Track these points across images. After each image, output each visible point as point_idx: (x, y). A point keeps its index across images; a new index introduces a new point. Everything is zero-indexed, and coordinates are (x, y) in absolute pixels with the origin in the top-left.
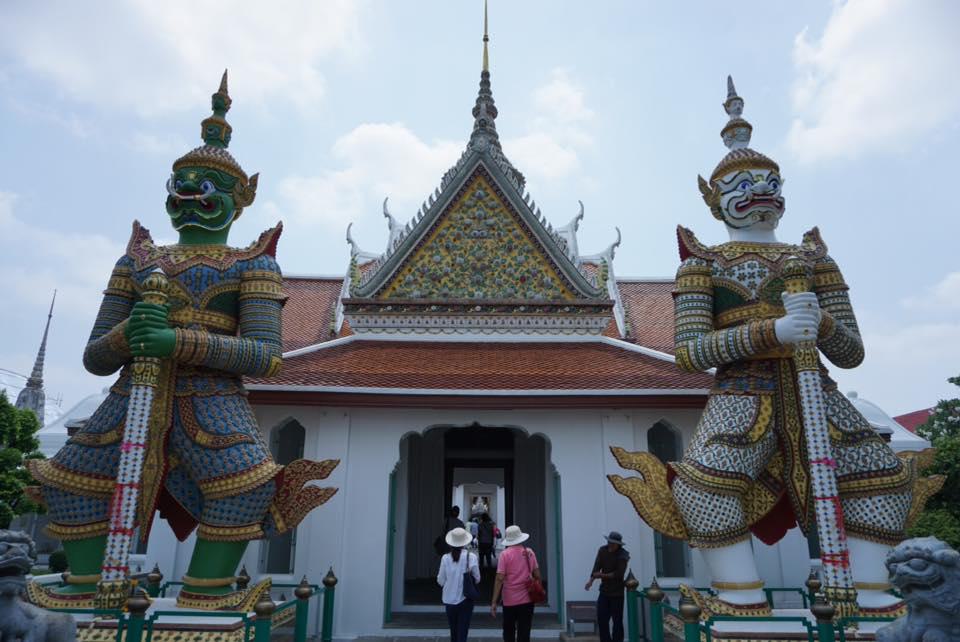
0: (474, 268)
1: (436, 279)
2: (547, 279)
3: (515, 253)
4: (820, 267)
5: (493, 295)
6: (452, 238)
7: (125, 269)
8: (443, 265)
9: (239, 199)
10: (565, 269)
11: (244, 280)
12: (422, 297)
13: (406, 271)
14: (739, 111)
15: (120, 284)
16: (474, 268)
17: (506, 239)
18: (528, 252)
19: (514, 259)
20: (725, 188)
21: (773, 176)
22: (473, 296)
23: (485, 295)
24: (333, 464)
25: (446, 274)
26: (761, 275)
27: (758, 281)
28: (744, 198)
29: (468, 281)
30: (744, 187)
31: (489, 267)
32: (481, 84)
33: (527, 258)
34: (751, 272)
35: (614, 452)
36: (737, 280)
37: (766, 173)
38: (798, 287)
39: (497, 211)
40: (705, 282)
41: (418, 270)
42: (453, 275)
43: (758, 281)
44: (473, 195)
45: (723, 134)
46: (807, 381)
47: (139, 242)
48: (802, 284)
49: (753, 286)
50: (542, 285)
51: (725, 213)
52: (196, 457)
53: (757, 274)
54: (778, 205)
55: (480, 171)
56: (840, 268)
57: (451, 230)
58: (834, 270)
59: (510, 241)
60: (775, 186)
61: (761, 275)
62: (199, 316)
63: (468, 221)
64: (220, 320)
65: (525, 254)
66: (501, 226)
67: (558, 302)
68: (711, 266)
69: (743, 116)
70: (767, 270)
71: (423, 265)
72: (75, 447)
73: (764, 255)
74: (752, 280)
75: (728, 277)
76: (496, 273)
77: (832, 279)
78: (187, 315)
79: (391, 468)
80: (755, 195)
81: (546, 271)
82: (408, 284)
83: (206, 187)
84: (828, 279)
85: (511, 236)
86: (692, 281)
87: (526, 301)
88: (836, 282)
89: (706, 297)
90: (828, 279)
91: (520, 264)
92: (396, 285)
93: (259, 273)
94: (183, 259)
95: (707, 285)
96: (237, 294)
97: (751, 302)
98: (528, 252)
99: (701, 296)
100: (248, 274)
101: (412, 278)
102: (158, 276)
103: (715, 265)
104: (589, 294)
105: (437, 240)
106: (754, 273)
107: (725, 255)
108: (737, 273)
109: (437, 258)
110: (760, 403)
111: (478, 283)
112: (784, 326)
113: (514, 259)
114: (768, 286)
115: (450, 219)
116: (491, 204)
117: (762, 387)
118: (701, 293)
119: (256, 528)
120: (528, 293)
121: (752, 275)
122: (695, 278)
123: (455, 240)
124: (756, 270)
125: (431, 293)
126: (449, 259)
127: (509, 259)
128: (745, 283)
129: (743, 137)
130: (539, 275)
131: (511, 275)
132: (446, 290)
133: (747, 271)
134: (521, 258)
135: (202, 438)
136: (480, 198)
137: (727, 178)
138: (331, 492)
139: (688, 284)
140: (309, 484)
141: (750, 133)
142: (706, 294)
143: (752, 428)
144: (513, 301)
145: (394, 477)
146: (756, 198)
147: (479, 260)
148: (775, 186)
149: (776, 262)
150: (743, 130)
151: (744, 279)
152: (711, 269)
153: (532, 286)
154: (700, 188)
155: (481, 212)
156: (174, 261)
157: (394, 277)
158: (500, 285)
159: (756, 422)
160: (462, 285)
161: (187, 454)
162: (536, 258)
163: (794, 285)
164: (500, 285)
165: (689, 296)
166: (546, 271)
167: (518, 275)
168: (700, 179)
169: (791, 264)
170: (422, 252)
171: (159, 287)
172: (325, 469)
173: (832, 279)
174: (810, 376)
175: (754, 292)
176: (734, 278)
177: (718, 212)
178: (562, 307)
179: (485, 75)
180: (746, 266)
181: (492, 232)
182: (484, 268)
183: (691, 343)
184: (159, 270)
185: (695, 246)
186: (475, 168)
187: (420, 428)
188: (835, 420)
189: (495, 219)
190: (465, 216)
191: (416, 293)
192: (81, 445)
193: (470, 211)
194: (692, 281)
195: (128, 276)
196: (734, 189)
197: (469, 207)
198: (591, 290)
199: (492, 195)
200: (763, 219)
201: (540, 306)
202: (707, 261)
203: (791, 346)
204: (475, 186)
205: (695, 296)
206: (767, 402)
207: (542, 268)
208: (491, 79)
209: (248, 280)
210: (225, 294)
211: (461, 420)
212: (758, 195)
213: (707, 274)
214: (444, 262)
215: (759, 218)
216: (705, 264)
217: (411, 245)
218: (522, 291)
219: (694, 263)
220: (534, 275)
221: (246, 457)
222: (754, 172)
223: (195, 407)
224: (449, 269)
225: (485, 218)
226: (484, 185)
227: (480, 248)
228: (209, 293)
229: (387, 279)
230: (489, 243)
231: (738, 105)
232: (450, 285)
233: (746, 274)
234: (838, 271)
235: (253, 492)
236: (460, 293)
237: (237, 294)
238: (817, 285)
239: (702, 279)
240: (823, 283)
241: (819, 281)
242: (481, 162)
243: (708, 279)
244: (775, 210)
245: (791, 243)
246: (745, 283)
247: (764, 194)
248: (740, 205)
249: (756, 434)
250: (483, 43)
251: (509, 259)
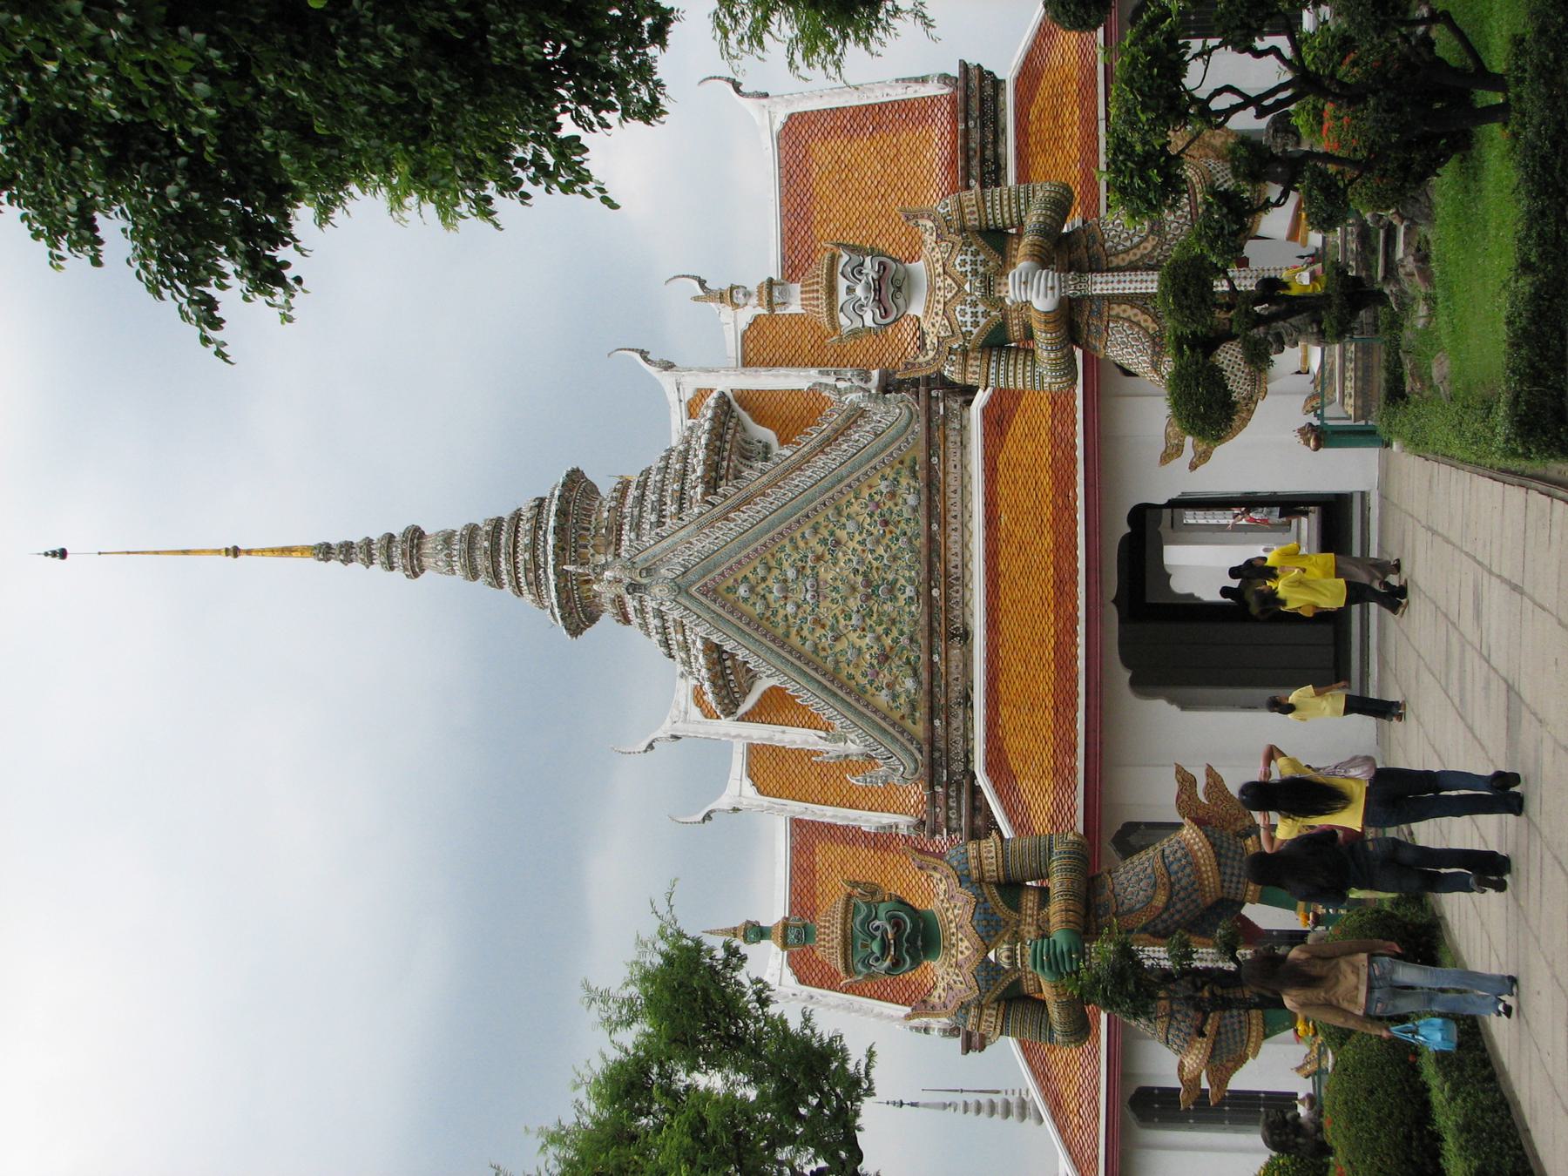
0: (868, 597)
1: (884, 658)
2: (883, 486)
4: (956, 225)
5: (910, 568)
6: (819, 632)
7: (973, 1012)
8: (863, 643)
9: (878, 897)
10: (869, 461)
11: (981, 880)
12: (915, 674)
14: (747, 295)
15: (990, 1015)
16: (868, 597)
17: (820, 549)
18: (840, 514)
19: (851, 536)
22: (910, 600)
23: (911, 581)
24: (1180, 771)
25: (878, 639)
26: (974, 304)
27: (981, 308)
29: (888, 607)
31: (865, 575)
32: (347, 560)
33: (849, 517)
35: (1166, 458)
37: (842, 284)
38: (1002, 288)
39: (773, 563)
40: (975, 359)
41: (871, 683)
42: (880, 630)
43: (981, 308)
44: (746, 600)
47: (933, 1007)
49: (986, 314)
50: (893, 495)
52: (1179, 906)
57: (805, 633)
59: (824, 542)
62: (1029, 920)
63: (790, 609)
64: (1030, 901)
65: (844, 520)
66: (796, 556)
67: (922, 474)
69: (753, 288)
71: (864, 675)
72: (1172, 1031)
73: (949, 296)
76: (875, 564)
77: (972, 213)
78: (1029, 931)
79: (1174, 709)
81: (870, 487)
82: (895, 697)
83: (877, 928)
87: (923, 522)
91: (860, 527)
92: (896, 715)
93: (973, 863)
94: (966, 943)
96: (998, 885)
97: (1004, 317)
98: (840, 514)
100: (975, 874)
101: (884, 692)
102: (999, 954)
104: (908, 425)
105: (823, 654)
110: (1118, 317)
111: (891, 591)
112: (1042, 302)
113: (851, 536)
115: (787, 635)
116: (761, 572)
117: (1100, 314)
119: (1249, 842)
120: (906, 515)
121: (974, 314)
123: (823, 626)
124: (969, 310)
125: (908, 662)
126: (853, 637)
127: (853, 544)
128: (982, 321)
130: (877, 498)
131: (878, 542)
132: (904, 641)
133: (968, 318)
134: (851, 526)
135: (1160, 899)
136: (752, 590)
138: (1210, 772)
140: (1203, 800)
143: (1146, 330)
144: (923, 539)
145: (1184, 706)
147: (854, 589)
153: (895, 509)
155: (775, 588)
156: (967, 953)
157: (885, 718)
158: (895, 558)
159: (1138, 324)
160: (894, 615)
161: (1177, 917)
164: (895, 558)
166: (870, 487)
167: (878, 530)
171: (1012, 951)
172: (1186, 781)
173: (972, 213)
174: (1099, 286)
176: (975, 331)
178: (930, 468)
179: (325, 552)
181: (809, 571)
182: (868, 583)
183: (1047, 380)
184: (991, 955)
186: (703, 599)
188: (1136, 239)
189: (786, 565)
190: (781, 613)
191: (909, 684)
192: (1170, 1024)
193: (773, 605)
195: (980, 1007)
197: (768, 607)
198: (903, 422)
200: (899, 289)
201: (930, 499)
203: (1061, 301)
204: (731, 596)
206: (1116, 310)
207: (866, 493)
208: (334, 540)
209: (982, 873)
210: (1002, 896)
211: (1112, 615)
214: (858, 643)
217: (835, 695)
218: (903, 525)
220: (877, 505)
221: (1179, 855)
222: (842, 296)
223: (1130, 911)
224: (870, 635)
225: (785, 581)
227: (835, 589)
228: (1003, 911)
229: (891, 730)
230: (827, 574)
232: (895, 633)
235: (1213, 845)
236: (906, 617)
237: (998, 885)
242: (693, 590)
246: (982, 321)
249: (1152, 326)
250: (242, 558)
251: (853, 544)
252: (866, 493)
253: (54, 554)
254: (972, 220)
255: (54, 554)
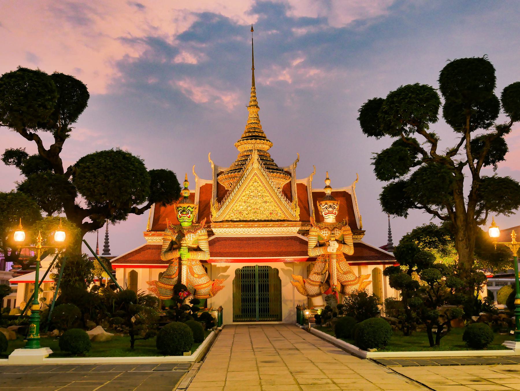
3: (268, 204)
13: (231, 212)
27: (327, 235)
43: (327, 235)
46: (334, 262)
55: (256, 174)
85: (267, 198)
109: (241, 207)
110: (325, 265)
126: (245, 207)
127: (266, 207)
138: (223, 287)
162: (275, 206)
170: (236, 204)
187: (240, 266)
199: (260, 183)
206: (327, 264)
207: (277, 209)
226: (257, 179)
230: (260, 201)
249: (323, 272)
252: (277, 209)
253: (252, 29)
255: (252, 29)
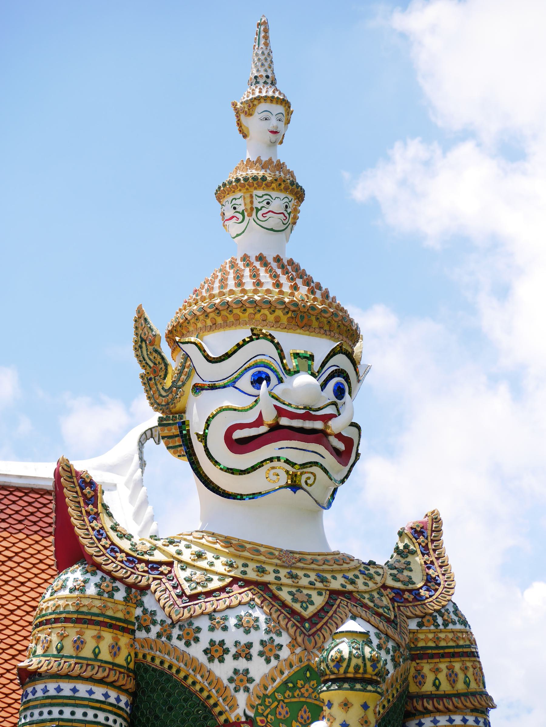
4: (426, 639)
20: (208, 372)
21: (341, 361)
28: (251, 417)
30: (257, 382)
34: (244, 639)
36: (203, 659)
37: (320, 346)
40: (115, 649)
43: (258, 668)
45: (221, 193)
48: (365, 706)
51: (198, 447)
53: (256, 648)
54: (341, 446)
56: (482, 650)
58: (466, 652)
60: (339, 392)
61: (269, 651)
68: (140, 604)
70: (284, 639)
73: (284, 595)
74: (242, 664)
75: (181, 645)
77: (452, 678)
80: (281, 412)
84: (442, 677)
86: (79, 644)
88: (460, 686)
89: (113, 694)
90: (442, 677)
95: (120, 660)
99: (99, 692)
103: (148, 601)
106: (249, 645)
107: (182, 575)
108: (205, 637)
114: (285, 683)
118: (101, 682)
121: (244, 651)
122: (90, 633)
124: (256, 637)
128: (223, 671)
129: (274, 221)
133: (233, 636)
137: (218, 342)
139: (69, 650)
141: (296, 210)
142: (112, 685)
146: (284, 421)
148: (339, 392)
149: (309, 620)
150: (279, 201)
151: (222, 660)
152: (138, 612)
154: (138, 348)
163: (346, 705)
165: (67, 688)
168: (141, 320)
169: (344, 648)
175: (242, 698)
176: (196, 651)
177: (176, 433)
180: (232, 621)
185: (100, 533)
194: (79, 644)
196: (233, 384)
202: (129, 587)
205: (83, 689)
212: (292, 416)
213: (124, 626)
215: (284, 479)
216: (120, 596)
219: (91, 590)
231: (273, 123)
233: (229, 644)
234: (474, 655)
238: (413, 689)
239: (108, 636)
240: (428, 687)
241: (420, 678)
243: (124, 640)
244: (329, 461)
245: (363, 555)
246: (223, 671)
247: (307, 416)
248: (238, 434)
254: (434, 677)
